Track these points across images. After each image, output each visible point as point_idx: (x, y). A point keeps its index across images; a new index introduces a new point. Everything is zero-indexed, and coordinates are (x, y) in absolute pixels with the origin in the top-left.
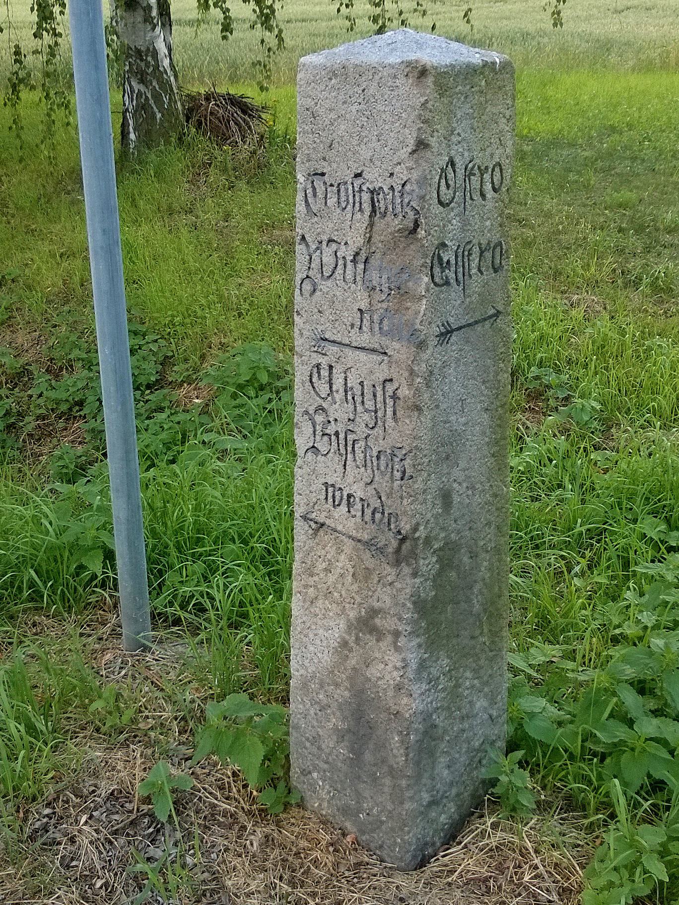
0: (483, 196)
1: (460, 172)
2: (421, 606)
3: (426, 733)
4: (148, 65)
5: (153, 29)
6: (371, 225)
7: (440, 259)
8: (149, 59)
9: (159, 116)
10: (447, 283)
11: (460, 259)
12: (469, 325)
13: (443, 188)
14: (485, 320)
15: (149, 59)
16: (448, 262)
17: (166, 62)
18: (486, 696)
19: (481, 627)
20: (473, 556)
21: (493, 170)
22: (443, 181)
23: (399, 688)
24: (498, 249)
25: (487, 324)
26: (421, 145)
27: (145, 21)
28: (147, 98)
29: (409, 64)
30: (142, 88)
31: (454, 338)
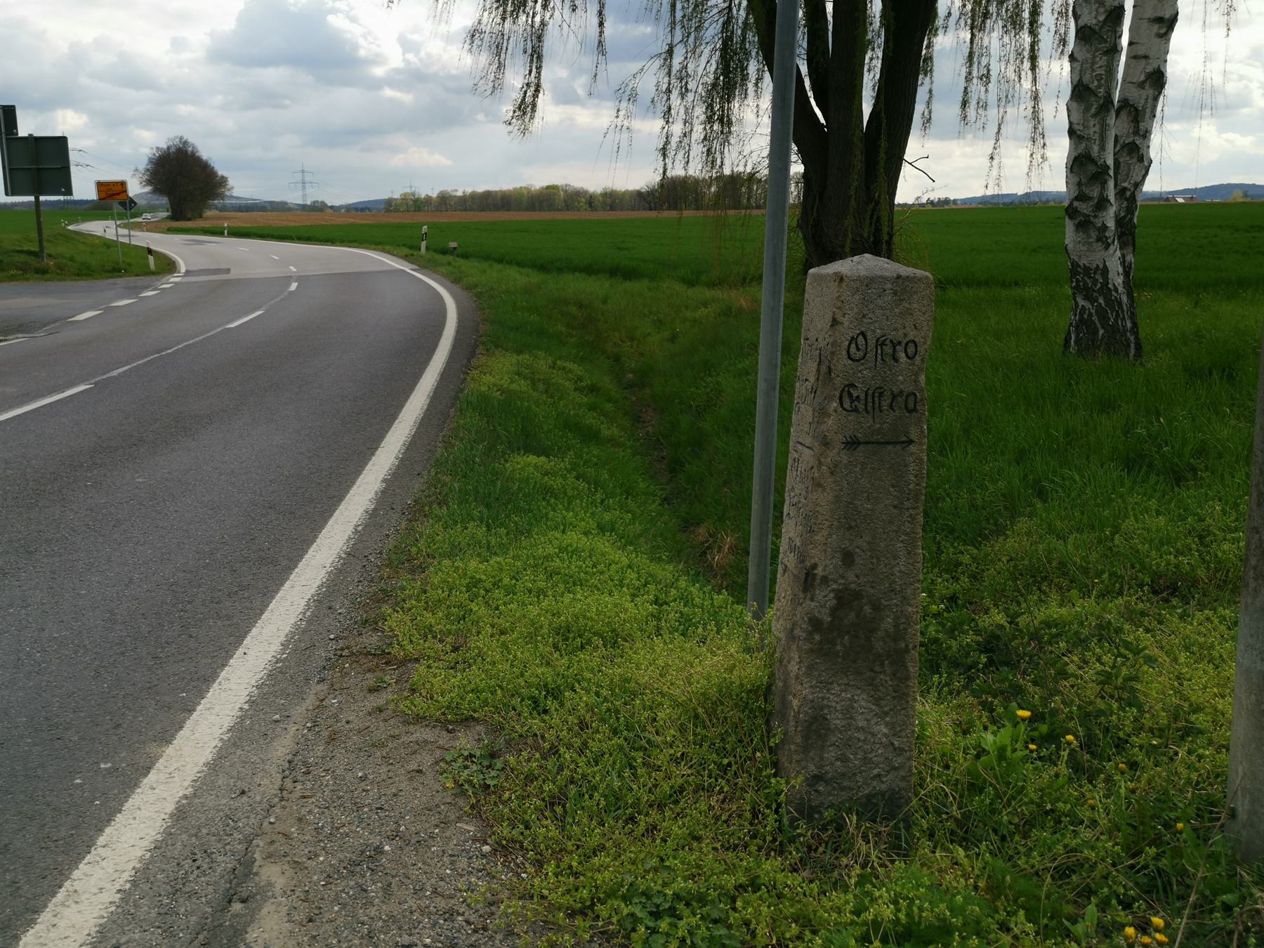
0: (896, 360)
1: (872, 343)
2: (816, 624)
3: (815, 718)
4: (1095, 282)
5: (1107, 247)
6: (818, 370)
7: (850, 395)
8: (1099, 277)
9: (1101, 332)
10: (856, 410)
11: (870, 400)
12: (878, 443)
13: (853, 349)
14: (896, 443)
15: (1099, 277)
16: (858, 397)
17: (1119, 281)
18: (887, 724)
19: (882, 664)
20: (876, 608)
21: (907, 344)
22: (853, 345)
23: (797, 677)
24: (912, 398)
25: (899, 447)
26: (835, 322)
27: (1098, 240)
28: (1090, 315)
29: (836, 274)
30: (1088, 305)
31: (861, 448)
